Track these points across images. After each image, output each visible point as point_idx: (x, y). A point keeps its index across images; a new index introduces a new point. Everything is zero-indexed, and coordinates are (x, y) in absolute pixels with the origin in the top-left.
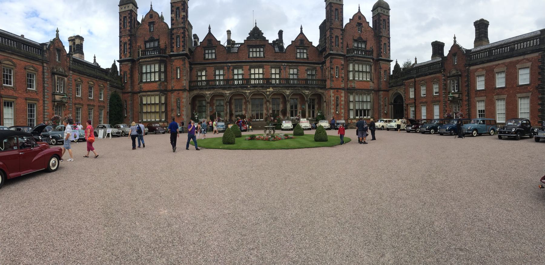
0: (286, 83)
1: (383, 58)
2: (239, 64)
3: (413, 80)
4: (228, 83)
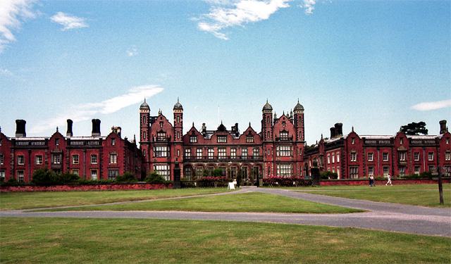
0: (240, 159)
2: (211, 147)
4: (205, 158)
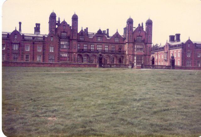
1: (149, 42)
3: (157, 52)
